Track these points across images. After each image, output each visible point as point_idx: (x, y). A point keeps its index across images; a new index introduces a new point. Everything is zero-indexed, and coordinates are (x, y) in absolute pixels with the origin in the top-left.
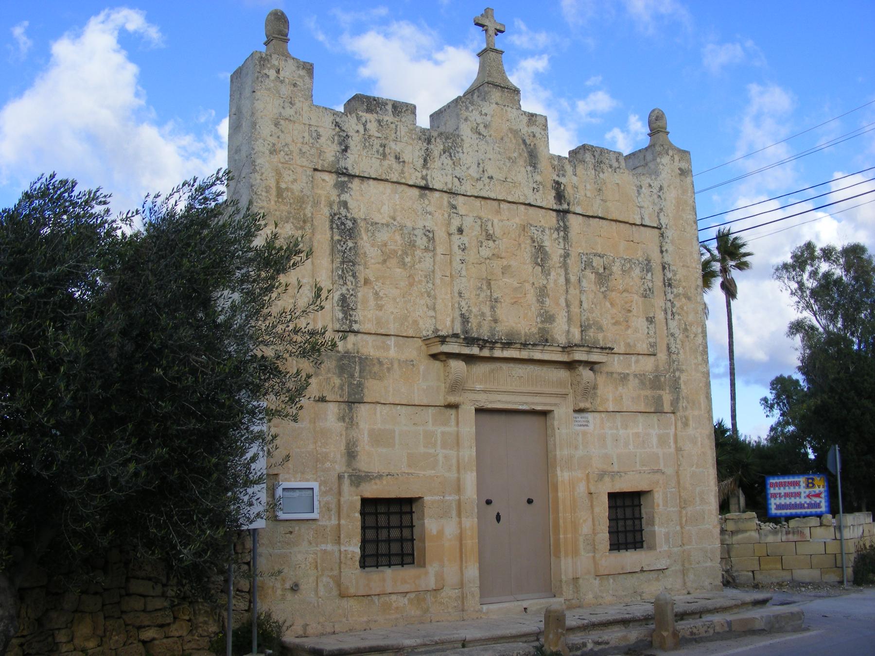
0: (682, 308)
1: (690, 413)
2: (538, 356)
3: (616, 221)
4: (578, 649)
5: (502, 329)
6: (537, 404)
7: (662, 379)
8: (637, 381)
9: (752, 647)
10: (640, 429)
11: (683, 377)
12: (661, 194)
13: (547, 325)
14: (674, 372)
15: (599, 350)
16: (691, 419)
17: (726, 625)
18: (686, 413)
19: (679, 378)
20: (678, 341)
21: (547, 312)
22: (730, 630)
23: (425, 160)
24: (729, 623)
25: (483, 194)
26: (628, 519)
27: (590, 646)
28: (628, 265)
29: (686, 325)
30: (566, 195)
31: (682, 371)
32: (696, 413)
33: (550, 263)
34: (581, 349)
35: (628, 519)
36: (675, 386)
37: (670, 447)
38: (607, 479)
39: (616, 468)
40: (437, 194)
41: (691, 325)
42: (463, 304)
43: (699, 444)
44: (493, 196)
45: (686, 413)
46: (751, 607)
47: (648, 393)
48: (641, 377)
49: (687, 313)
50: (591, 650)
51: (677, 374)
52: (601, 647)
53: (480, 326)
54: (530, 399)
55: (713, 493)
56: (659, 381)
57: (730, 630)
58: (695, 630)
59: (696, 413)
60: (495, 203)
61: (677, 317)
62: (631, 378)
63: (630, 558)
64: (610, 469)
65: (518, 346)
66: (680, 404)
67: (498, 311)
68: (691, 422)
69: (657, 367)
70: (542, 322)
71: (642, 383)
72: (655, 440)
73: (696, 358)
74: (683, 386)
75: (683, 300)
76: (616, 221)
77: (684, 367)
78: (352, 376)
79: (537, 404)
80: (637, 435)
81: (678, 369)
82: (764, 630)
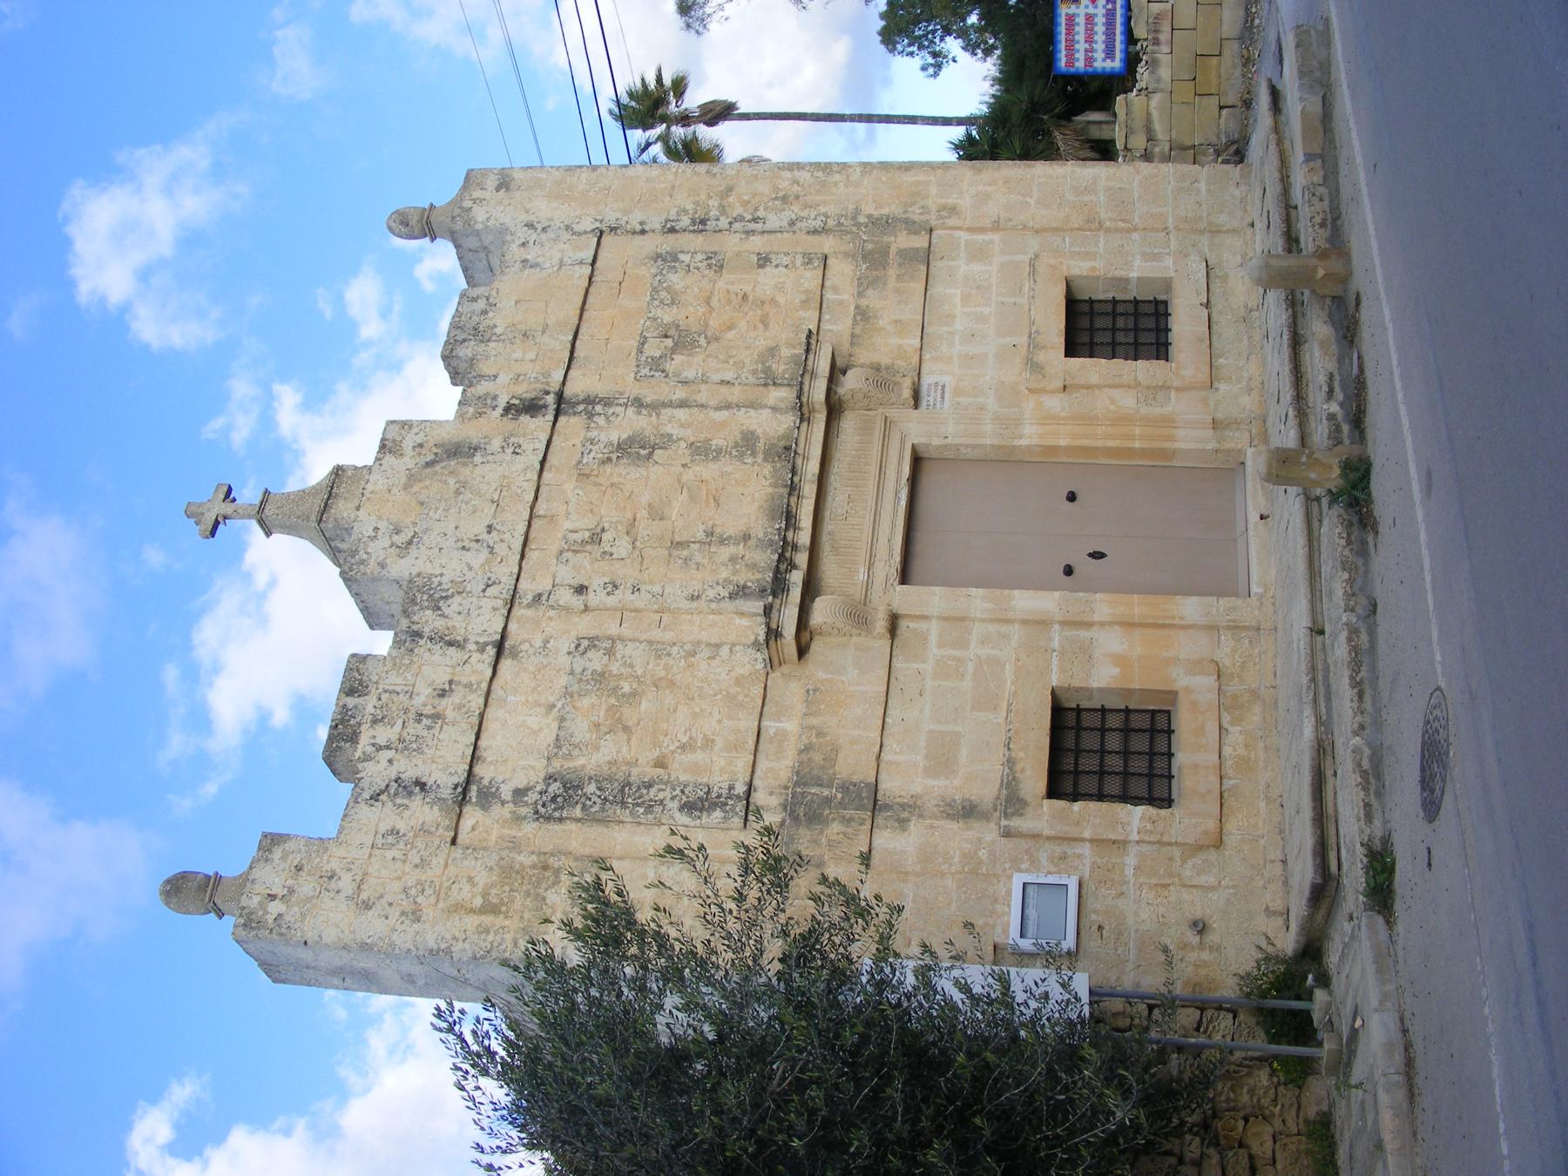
0: (745, 204)
2: (813, 467)
3: (582, 309)
4: (1338, 429)
5: (763, 527)
6: (899, 472)
7: (870, 246)
8: (870, 292)
9: (1352, 121)
10: (956, 292)
11: (869, 209)
12: (539, 227)
13: (760, 445)
14: (858, 225)
15: (811, 357)
16: (943, 201)
17: (1312, 164)
18: (933, 207)
19: (870, 216)
20: (804, 214)
21: (736, 445)
22: (1321, 156)
23: (450, 644)
24: (1309, 157)
26: (1113, 325)
27: (1334, 407)
28: (663, 294)
30: (529, 396)
31: (857, 211)
32: (933, 190)
35: (1113, 325)
36: (884, 224)
37: (992, 241)
38: (1041, 357)
39: (1023, 340)
40: (512, 627)
41: (777, 189)
42: (711, 594)
43: (989, 189)
44: (522, 528)
45: (933, 207)
46: (1283, 118)
47: (892, 273)
48: (863, 285)
50: (1341, 405)
51: (862, 219)
52: (1337, 389)
53: (753, 566)
54: (890, 485)
55: (1078, 170)
56: (871, 252)
57: (1321, 156)
58: (1318, 220)
59: (933, 190)
60: (536, 524)
61: (761, 214)
62: (863, 302)
63: (1184, 325)
64: (1024, 351)
65: (793, 500)
66: (917, 218)
67: (730, 532)
68: (950, 201)
69: (846, 255)
70: (754, 454)
71: (873, 283)
72: (977, 268)
73: (836, 184)
74: (885, 211)
75: (731, 199)
76: (582, 309)
77: (852, 207)
78: (828, 801)
79: (899, 472)
80: (966, 298)
81: (854, 218)
82: (1324, 98)
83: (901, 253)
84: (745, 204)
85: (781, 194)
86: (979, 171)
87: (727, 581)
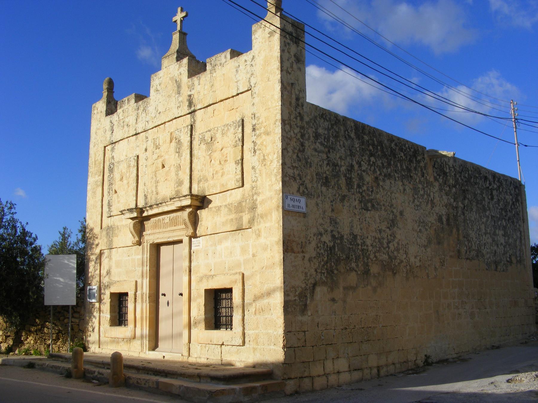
0: (262, 144)
1: (262, 226)
2: (166, 209)
3: (222, 101)
4: (92, 374)
5: (160, 197)
6: (174, 236)
7: (244, 204)
8: (226, 209)
9: (104, 394)
11: (259, 199)
12: (253, 63)
13: (179, 188)
14: (253, 196)
15: (183, 198)
17: (155, 383)
18: (259, 227)
19: (256, 200)
20: (257, 171)
21: (179, 180)
22: (157, 388)
23: (137, 120)
24: (158, 383)
25: (157, 124)
26: (218, 308)
27: (96, 374)
28: (226, 129)
29: (264, 156)
30: (194, 101)
31: (258, 194)
32: (268, 225)
33: (183, 148)
34: (175, 200)
35: (218, 308)
36: (253, 208)
38: (205, 280)
39: (212, 273)
40: (142, 134)
42: (145, 189)
44: (160, 123)
46: (209, 380)
47: (233, 216)
48: (229, 207)
49: (265, 146)
50: (96, 376)
51: (255, 198)
52: (101, 376)
53: (151, 199)
54: (171, 234)
56: (241, 206)
57: (157, 388)
58: (139, 381)
59: (268, 225)
61: (258, 152)
62: (223, 209)
64: (210, 274)
65: (155, 206)
67: (159, 188)
68: (263, 233)
69: (244, 195)
70: (177, 186)
71: (230, 210)
73: (271, 180)
74: (258, 206)
76: (222, 101)
77: (260, 191)
79: (174, 236)
81: (256, 193)
82: (179, 395)
83: (241, 217)
84: (262, 144)
85: (266, 157)
86: (277, 243)
87: (148, 192)
